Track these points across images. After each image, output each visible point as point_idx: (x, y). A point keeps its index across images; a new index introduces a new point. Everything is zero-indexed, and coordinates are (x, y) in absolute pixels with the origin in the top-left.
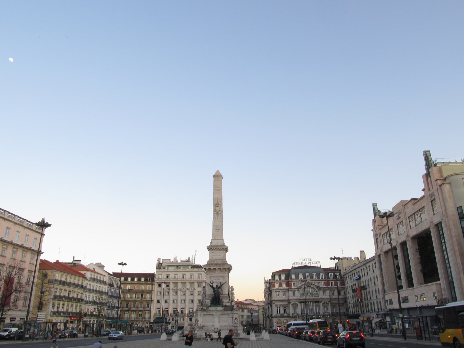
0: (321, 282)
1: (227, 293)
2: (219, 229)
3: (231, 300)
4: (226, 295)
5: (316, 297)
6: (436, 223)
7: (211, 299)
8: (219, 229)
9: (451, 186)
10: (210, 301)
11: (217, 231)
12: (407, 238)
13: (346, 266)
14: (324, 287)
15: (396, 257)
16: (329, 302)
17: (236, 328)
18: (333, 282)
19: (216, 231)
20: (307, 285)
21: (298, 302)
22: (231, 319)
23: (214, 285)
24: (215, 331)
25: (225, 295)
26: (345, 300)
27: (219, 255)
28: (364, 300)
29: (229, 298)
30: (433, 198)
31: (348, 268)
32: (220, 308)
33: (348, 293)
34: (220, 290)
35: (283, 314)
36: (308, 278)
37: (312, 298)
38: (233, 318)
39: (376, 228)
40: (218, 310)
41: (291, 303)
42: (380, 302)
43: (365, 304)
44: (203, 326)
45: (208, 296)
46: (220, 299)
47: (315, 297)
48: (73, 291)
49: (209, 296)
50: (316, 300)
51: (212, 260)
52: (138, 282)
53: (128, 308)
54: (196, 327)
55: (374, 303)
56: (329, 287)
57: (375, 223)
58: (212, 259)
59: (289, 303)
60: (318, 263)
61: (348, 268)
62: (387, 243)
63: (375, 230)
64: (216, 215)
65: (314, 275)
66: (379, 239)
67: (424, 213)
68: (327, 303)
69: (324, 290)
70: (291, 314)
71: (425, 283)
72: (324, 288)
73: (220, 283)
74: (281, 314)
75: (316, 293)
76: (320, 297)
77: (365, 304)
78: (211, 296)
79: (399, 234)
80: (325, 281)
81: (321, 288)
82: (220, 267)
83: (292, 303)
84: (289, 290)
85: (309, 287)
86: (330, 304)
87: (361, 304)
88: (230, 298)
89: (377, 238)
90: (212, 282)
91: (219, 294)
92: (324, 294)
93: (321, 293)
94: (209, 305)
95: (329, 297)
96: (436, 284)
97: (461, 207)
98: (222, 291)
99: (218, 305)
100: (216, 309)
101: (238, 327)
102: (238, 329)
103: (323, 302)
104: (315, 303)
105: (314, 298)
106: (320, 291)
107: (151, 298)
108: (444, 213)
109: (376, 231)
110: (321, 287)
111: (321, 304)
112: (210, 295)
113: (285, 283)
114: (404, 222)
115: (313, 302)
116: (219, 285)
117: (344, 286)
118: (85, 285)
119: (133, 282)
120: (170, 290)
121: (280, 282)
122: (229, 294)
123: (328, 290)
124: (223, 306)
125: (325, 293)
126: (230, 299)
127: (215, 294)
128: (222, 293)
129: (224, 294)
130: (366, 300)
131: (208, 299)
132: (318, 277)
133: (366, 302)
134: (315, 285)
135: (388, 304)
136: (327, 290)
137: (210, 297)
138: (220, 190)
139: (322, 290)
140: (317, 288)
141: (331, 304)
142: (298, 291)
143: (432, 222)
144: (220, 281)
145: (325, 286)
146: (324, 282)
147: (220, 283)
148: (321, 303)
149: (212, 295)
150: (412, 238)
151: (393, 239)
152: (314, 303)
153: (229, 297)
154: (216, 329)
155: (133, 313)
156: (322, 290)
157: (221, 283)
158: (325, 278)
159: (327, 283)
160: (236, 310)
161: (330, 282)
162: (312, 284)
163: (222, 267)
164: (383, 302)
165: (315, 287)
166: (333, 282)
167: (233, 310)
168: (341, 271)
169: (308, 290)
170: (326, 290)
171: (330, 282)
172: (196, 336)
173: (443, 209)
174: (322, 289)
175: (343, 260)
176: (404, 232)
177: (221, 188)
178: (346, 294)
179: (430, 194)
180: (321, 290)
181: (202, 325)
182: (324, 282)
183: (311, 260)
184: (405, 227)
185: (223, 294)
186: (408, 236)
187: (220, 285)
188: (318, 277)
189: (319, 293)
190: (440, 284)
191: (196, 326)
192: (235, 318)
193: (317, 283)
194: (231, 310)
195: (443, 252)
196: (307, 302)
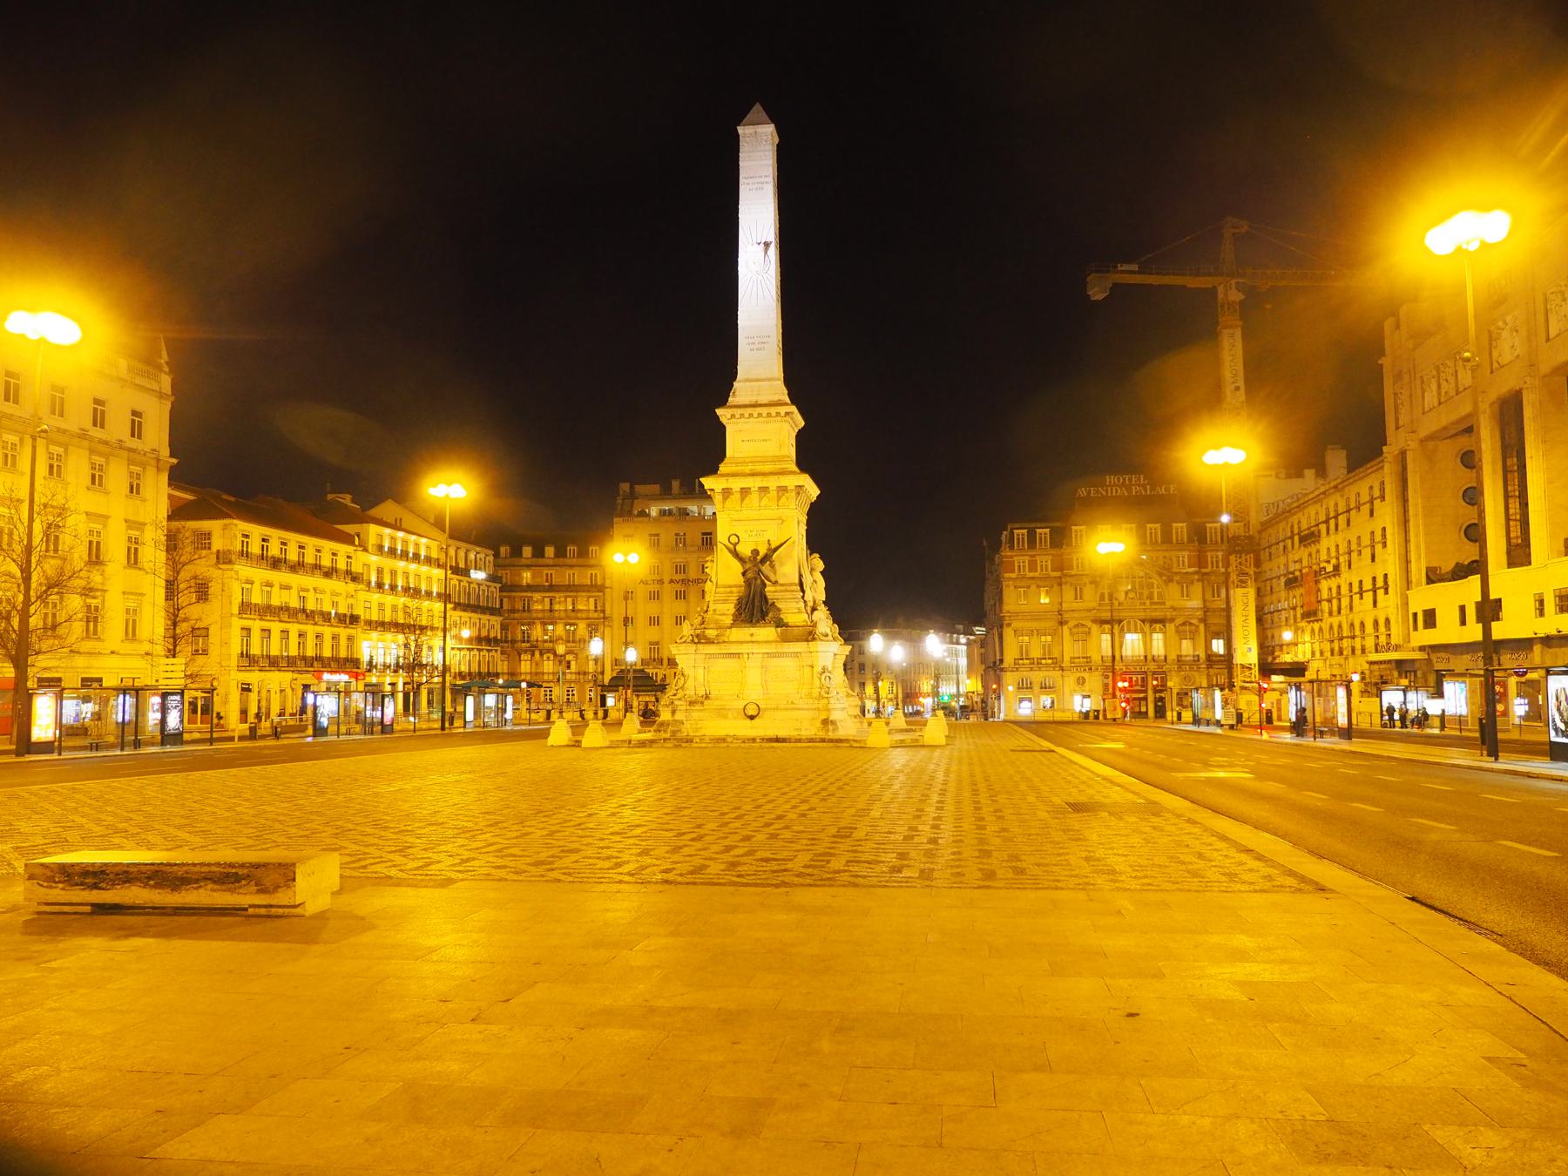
1: (797, 581)
3: (810, 604)
4: (791, 584)
5: (1157, 603)
7: (734, 598)
8: (765, 340)
13: (1272, 501)
14: (1185, 571)
15: (1469, 460)
17: (825, 701)
21: (1094, 621)
22: (808, 670)
23: (745, 550)
24: (751, 712)
25: (782, 585)
28: (1326, 615)
29: (803, 597)
31: (1276, 505)
32: (766, 632)
33: (1269, 592)
34: (766, 568)
35: (1038, 659)
38: (815, 670)
40: (759, 639)
41: (1066, 623)
42: (1387, 621)
43: (1331, 627)
44: (707, 697)
45: (722, 590)
46: (764, 598)
47: (1152, 603)
48: (315, 589)
49: (728, 590)
52: (533, 560)
53: (528, 645)
54: (680, 699)
55: (1362, 625)
56: (1203, 570)
59: (1061, 623)
61: (1278, 506)
64: (750, 285)
68: (1191, 624)
69: (1185, 581)
70: (1067, 658)
73: (769, 541)
74: (1033, 659)
76: (1169, 604)
77: (1331, 627)
78: (734, 590)
79: (1495, 365)
80: (1190, 551)
83: (1071, 624)
84: (1063, 580)
86: (1202, 627)
87: (1316, 626)
88: (806, 598)
90: (734, 539)
91: (762, 581)
92: (1183, 596)
94: (728, 620)
98: (775, 573)
99: (758, 622)
100: (752, 635)
101: (832, 701)
102: (830, 706)
103: (1179, 621)
104: (1151, 626)
106: (1170, 584)
107: (603, 611)
110: (1174, 570)
112: (730, 587)
113: (1050, 558)
116: (763, 552)
118: (361, 571)
119: (541, 561)
120: (663, 583)
121: (1032, 556)
122: (801, 584)
123: (1198, 580)
124: (780, 623)
125: (1187, 591)
126: (805, 602)
127: (748, 583)
128: (773, 580)
129: (780, 582)
130: (1335, 613)
131: (725, 601)
133: (1335, 621)
135: (1416, 628)
136: (1195, 582)
137: (731, 592)
141: (1206, 625)
142: (1093, 586)
144: (767, 536)
145: (1189, 567)
147: (769, 541)
148: (1173, 624)
149: (740, 586)
151: (1465, 389)
152: (1148, 625)
153: (802, 594)
154: (754, 707)
155: (548, 658)
156: (1178, 583)
157: (771, 542)
160: (826, 638)
164: (1398, 622)
167: (814, 639)
170: (1192, 582)
172: (680, 731)
174: (1177, 578)
176: (1516, 355)
180: (1175, 582)
181: (702, 692)
185: (775, 583)
187: (769, 549)
191: (679, 696)
192: (820, 669)
194: (807, 641)
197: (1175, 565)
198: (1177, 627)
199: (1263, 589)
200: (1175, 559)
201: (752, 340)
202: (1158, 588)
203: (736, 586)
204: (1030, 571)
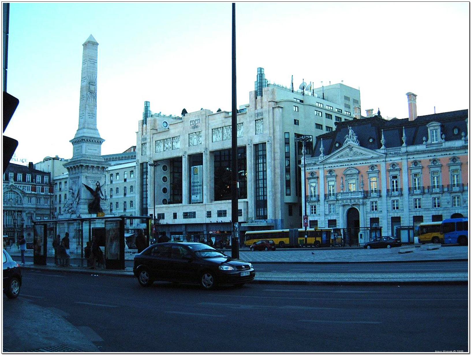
0: (27, 186)
2: (93, 116)
6: (255, 144)
8: (93, 115)
9: (282, 111)
10: (87, 206)
11: (92, 118)
12: (206, 151)
16: (34, 212)
18: (41, 187)
19: (90, 118)
20: (9, 189)
26: (52, 210)
27: (95, 150)
30: (260, 117)
36: (12, 180)
37: (15, 206)
39: (144, 131)
49: (85, 200)
50: (19, 209)
51: (87, 155)
57: (145, 125)
58: (86, 154)
60: (24, 161)
62: (162, 150)
63: (142, 134)
65: (20, 176)
66: (148, 145)
67: (240, 129)
71: (216, 200)
72: (31, 194)
75: (19, 199)
78: (87, 200)
81: (27, 194)
82: (99, 165)
85: (11, 191)
89: (143, 142)
93: (25, 200)
95: (35, 206)
96: (244, 202)
97: (289, 133)
105: (17, 205)
106: (25, 197)
108: (272, 135)
109: (144, 134)
111: (24, 214)
112: (85, 199)
114: (203, 134)
115: (14, 211)
117: (53, 194)
132: (24, 179)
134: (20, 190)
138: (95, 63)
139: (27, 196)
140: (22, 194)
143: (251, 141)
145: (32, 191)
146: (30, 186)
150: (210, 152)
156: (27, 196)
158: (32, 181)
159: (34, 189)
161: (37, 187)
162: (15, 188)
163: (100, 166)
165: (19, 192)
166: (41, 187)
168: (50, 174)
169: (9, 195)
170: (32, 197)
171: (37, 187)
173: (272, 131)
174: (28, 195)
175: (55, 160)
177: (95, 61)
178: (53, 203)
179: (256, 112)
182: (30, 186)
183: (16, 156)
184: (204, 138)
186: (206, 149)
188: (24, 179)
189: (23, 199)
190: (247, 202)
193: (22, 187)
195: (257, 172)
196: (7, 210)
197: (27, 190)
198: (26, 214)
199: (54, 201)
200: (27, 188)
201: (90, 115)
202: (20, 198)
203: (87, 199)
204: (42, 192)
